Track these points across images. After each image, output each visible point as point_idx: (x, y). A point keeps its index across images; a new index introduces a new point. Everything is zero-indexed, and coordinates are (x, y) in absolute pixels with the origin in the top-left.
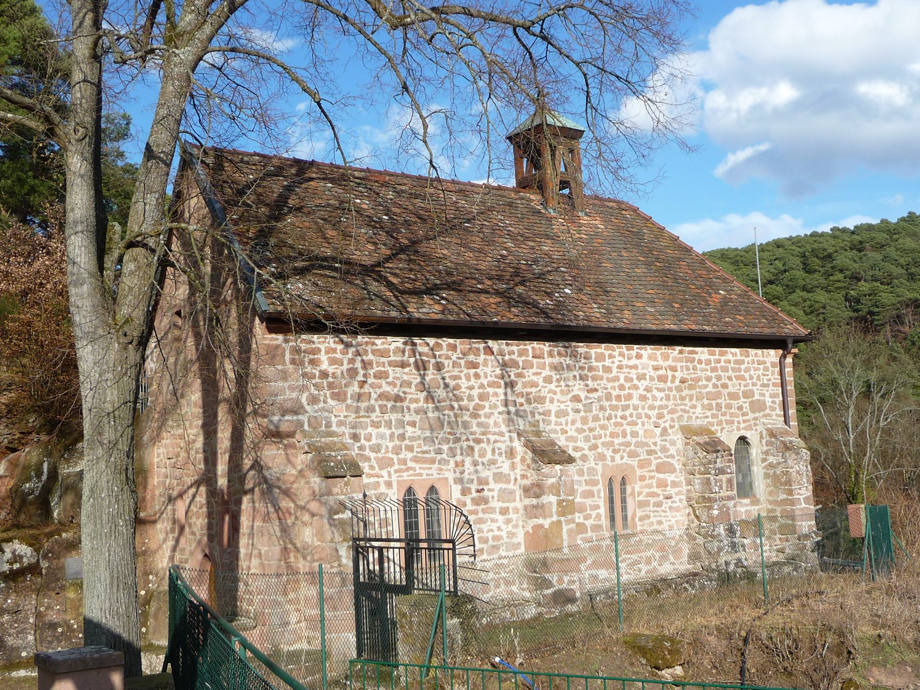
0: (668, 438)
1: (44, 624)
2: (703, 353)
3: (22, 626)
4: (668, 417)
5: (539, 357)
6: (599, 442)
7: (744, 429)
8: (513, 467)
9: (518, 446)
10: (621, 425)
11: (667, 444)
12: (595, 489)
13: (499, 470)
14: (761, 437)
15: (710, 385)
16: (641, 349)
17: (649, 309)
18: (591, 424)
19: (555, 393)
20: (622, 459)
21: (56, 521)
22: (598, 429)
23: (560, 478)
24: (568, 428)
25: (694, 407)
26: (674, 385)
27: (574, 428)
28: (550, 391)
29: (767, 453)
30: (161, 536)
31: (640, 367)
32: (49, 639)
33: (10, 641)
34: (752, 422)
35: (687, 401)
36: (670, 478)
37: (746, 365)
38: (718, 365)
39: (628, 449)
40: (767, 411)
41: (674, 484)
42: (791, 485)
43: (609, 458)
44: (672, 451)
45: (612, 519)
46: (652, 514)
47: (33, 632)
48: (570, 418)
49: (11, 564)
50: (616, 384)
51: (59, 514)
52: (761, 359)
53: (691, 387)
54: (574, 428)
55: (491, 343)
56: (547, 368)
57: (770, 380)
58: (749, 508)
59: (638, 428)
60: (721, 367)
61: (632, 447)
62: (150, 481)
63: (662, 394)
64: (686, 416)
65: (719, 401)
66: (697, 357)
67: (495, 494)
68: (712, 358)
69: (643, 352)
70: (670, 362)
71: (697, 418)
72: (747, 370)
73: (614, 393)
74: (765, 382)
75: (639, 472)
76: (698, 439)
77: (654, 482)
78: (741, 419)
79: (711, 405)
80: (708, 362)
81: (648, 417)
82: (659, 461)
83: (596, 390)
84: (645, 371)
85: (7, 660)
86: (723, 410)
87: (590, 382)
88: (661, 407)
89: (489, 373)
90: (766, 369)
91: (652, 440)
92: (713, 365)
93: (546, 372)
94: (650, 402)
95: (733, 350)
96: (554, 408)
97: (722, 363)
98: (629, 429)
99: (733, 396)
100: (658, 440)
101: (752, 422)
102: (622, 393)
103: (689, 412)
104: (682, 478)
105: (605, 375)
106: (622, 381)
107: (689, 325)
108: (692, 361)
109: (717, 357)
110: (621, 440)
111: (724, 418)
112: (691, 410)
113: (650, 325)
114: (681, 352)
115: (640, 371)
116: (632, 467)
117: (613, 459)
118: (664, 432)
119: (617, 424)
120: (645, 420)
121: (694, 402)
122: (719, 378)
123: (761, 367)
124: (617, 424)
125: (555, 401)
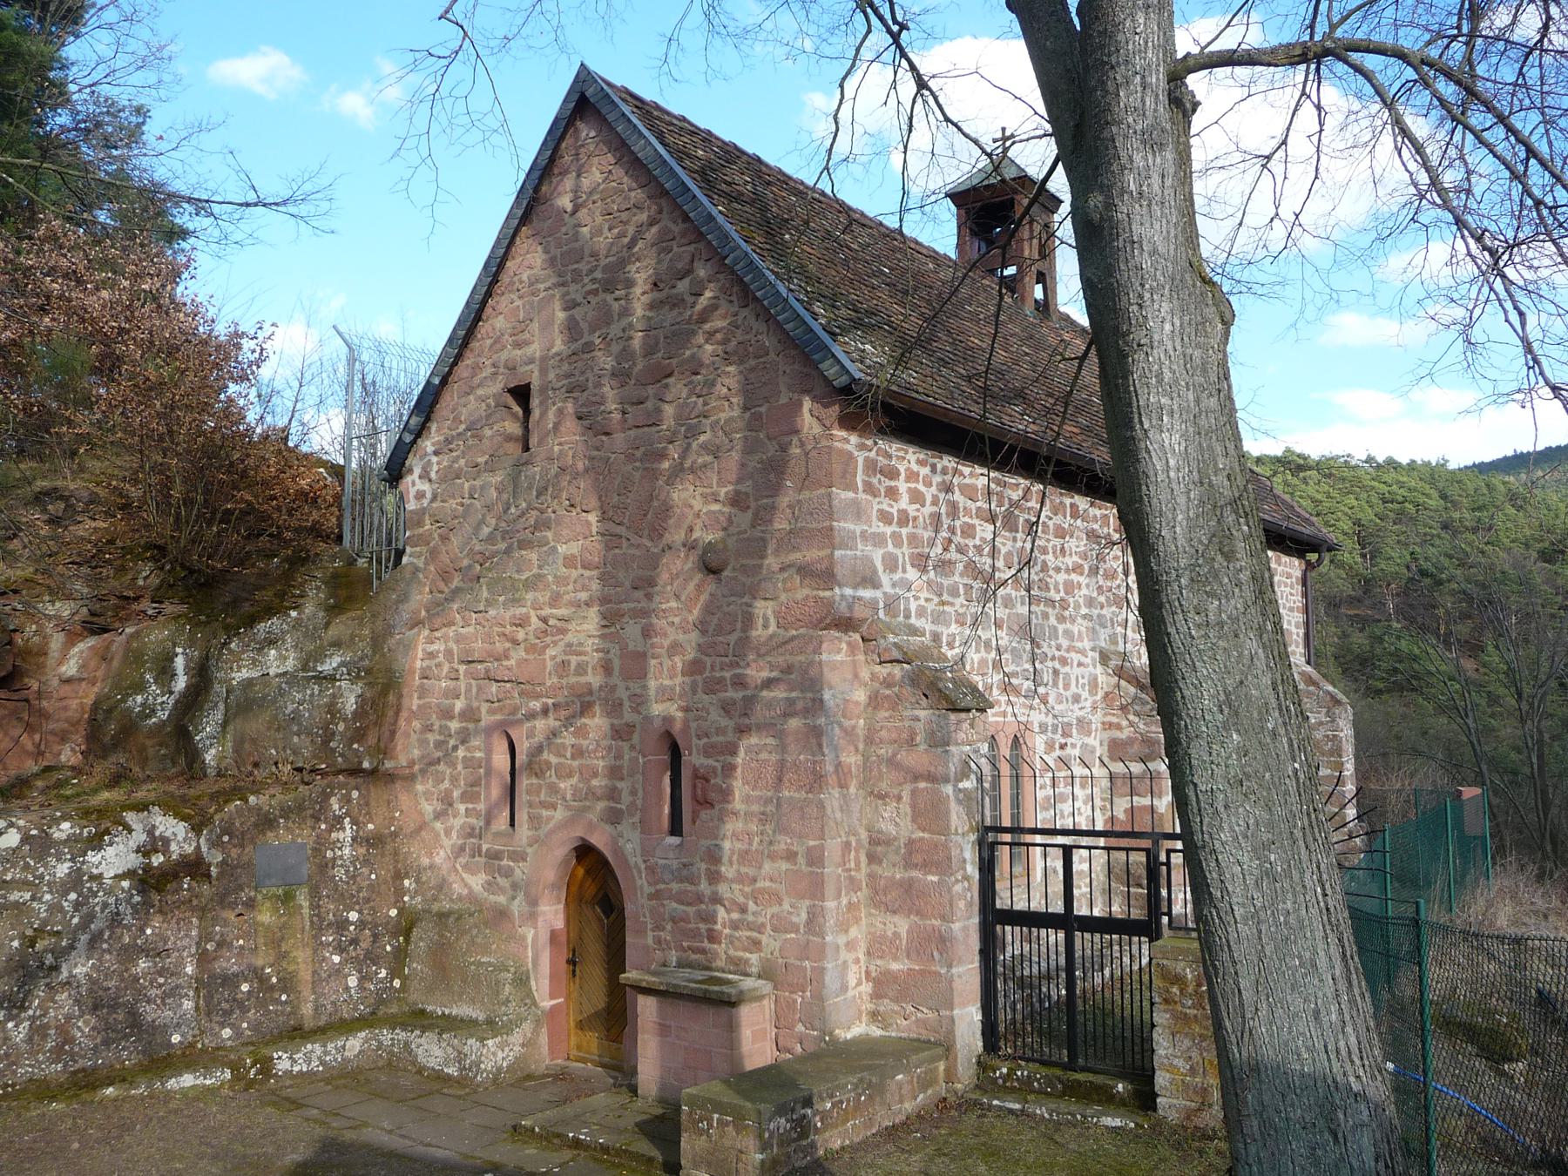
1: (212, 976)
3: (173, 981)
21: (211, 772)
30: (428, 808)
32: (225, 1005)
33: (149, 1012)
42: (1341, 756)
47: (191, 993)
49: (146, 854)
51: (220, 758)
62: (405, 702)
85: (144, 1052)
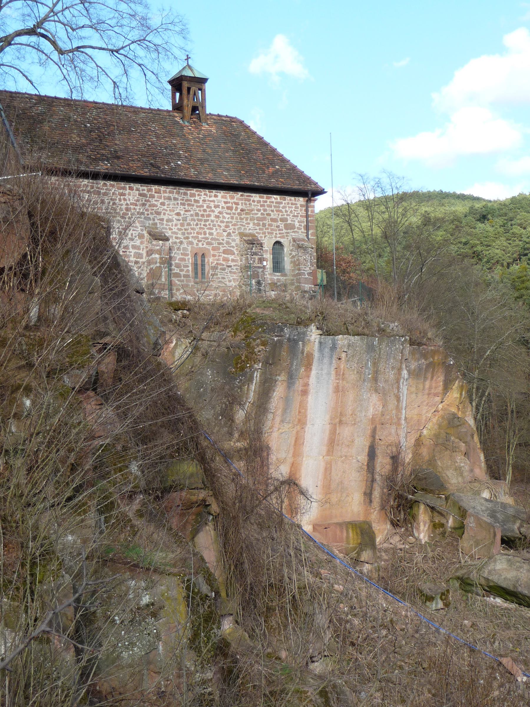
0: (231, 238)
2: (256, 197)
4: (231, 227)
5: (158, 193)
6: (190, 236)
7: (279, 237)
8: (142, 243)
9: (145, 233)
10: (204, 229)
11: (230, 241)
12: (187, 258)
13: (135, 244)
14: (290, 243)
15: (260, 213)
16: (217, 192)
17: (224, 173)
18: (186, 227)
19: (166, 210)
20: (203, 245)
22: (190, 229)
23: (162, 247)
24: (173, 228)
25: (249, 224)
26: (237, 212)
27: (176, 228)
28: (164, 209)
29: (292, 250)
31: (216, 202)
34: (285, 234)
35: (244, 220)
36: (231, 257)
37: (283, 205)
38: (266, 204)
39: (207, 241)
40: (296, 230)
41: (233, 260)
43: (195, 244)
44: (233, 244)
45: (196, 273)
46: (219, 274)
48: (174, 223)
50: (202, 209)
52: (294, 202)
53: (247, 214)
54: (176, 228)
55: (132, 185)
56: (163, 198)
57: (299, 213)
58: (279, 278)
59: (214, 231)
60: (267, 205)
61: (209, 240)
63: (229, 216)
64: (243, 228)
65: (264, 222)
66: (252, 199)
67: (132, 254)
68: (261, 200)
69: (218, 194)
70: (235, 200)
71: (250, 229)
72: (284, 207)
73: (200, 213)
74: (296, 214)
75: (212, 252)
76: (246, 238)
77: (221, 258)
78: (278, 232)
79: (259, 224)
80: (259, 202)
81: (220, 226)
82: (225, 248)
83: (190, 211)
84: (219, 204)
86: (267, 227)
87: (186, 207)
88: (227, 222)
89: (131, 199)
90: (296, 208)
91: (222, 238)
92: (262, 203)
93: (161, 201)
94: (221, 219)
95: (275, 196)
96: (165, 217)
97: (268, 203)
98: (208, 231)
99: (273, 220)
100: (225, 238)
101: (285, 234)
102: (205, 213)
103: (245, 226)
104: (239, 258)
105: (195, 204)
106: (205, 208)
107: (246, 182)
108: (249, 200)
109: (265, 199)
110: (203, 236)
111: (267, 231)
112: (247, 225)
113: (221, 181)
114: (242, 195)
115: (216, 203)
116: (208, 250)
117: (197, 244)
118: (229, 234)
119: (200, 228)
120: (218, 228)
121: (249, 221)
122: (265, 210)
123: (294, 206)
124: (200, 228)
125: (166, 215)
